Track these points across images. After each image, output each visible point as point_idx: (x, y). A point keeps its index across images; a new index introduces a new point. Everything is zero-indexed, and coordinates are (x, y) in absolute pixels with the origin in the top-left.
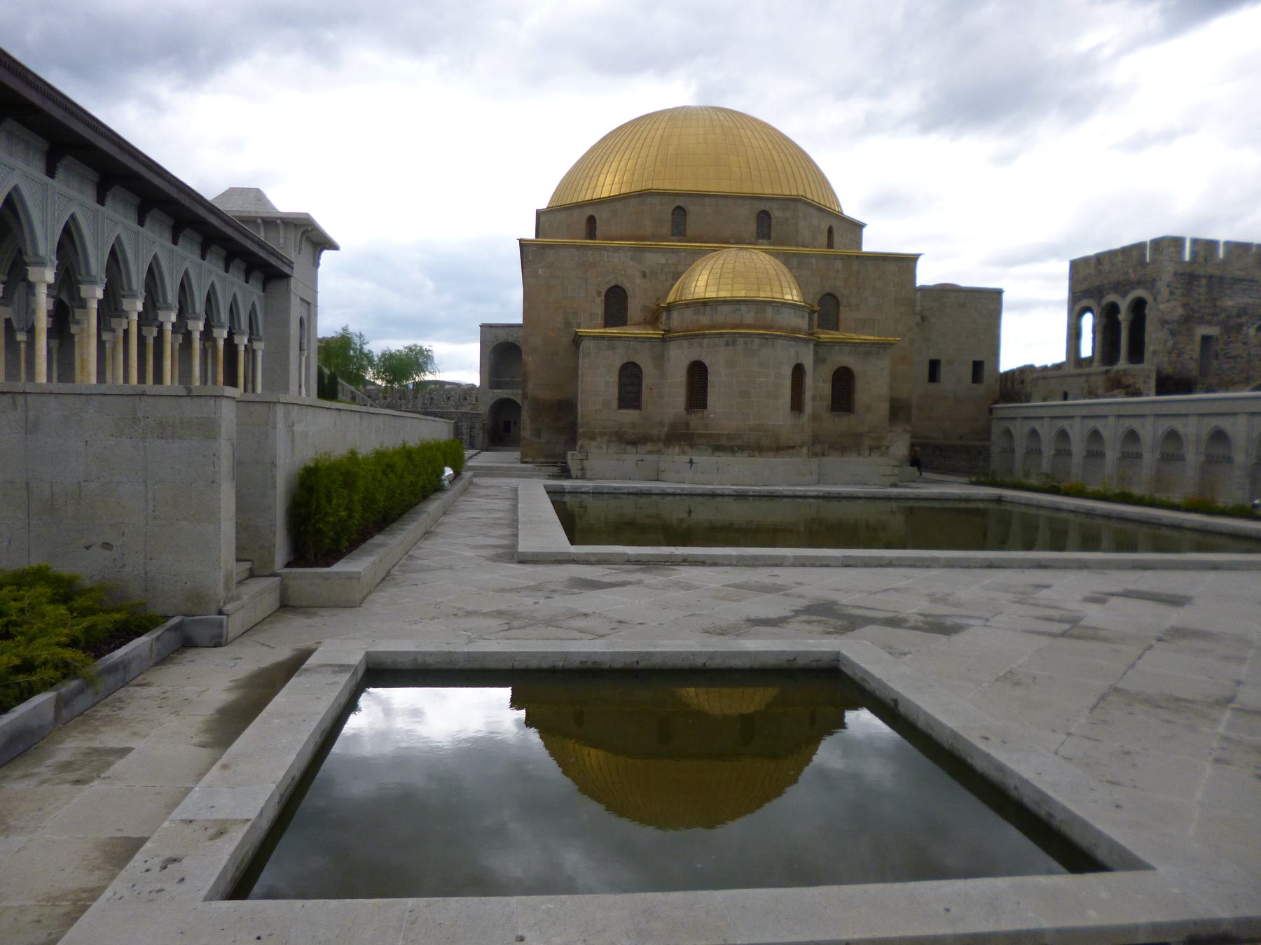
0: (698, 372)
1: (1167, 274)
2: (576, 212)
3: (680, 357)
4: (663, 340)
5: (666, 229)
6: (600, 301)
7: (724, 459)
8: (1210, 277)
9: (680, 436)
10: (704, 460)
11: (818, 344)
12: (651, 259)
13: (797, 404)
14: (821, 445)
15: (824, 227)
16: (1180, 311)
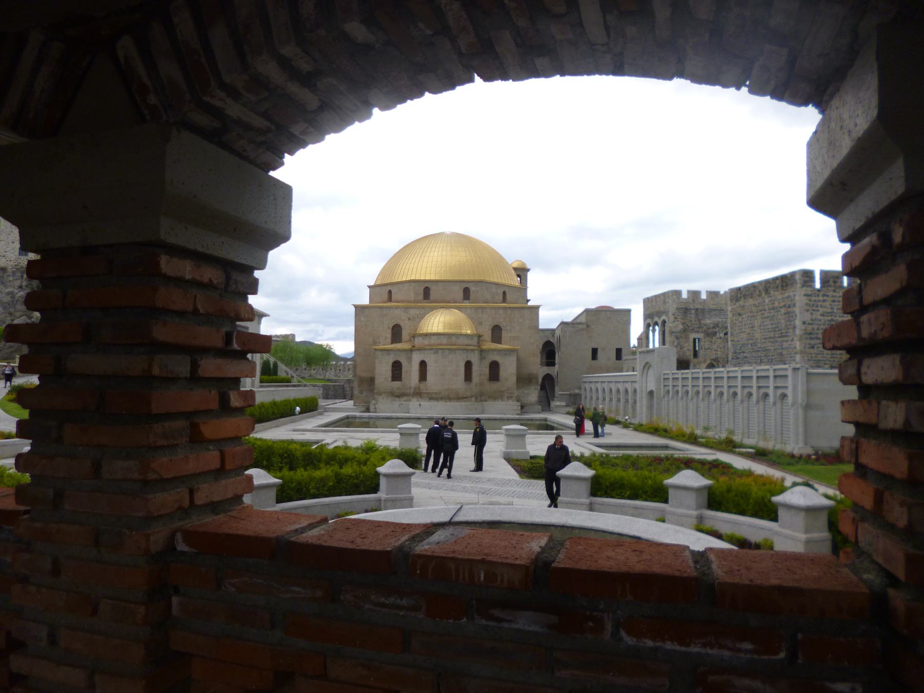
0: (423, 364)
1: (672, 307)
2: (384, 288)
3: (417, 358)
4: (411, 350)
5: (421, 297)
6: (389, 331)
7: (434, 403)
8: (697, 309)
9: (418, 394)
10: (426, 404)
11: (482, 351)
12: (413, 312)
13: (468, 377)
14: (481, 397)
15: (500, 291)
16: (681, 327)
